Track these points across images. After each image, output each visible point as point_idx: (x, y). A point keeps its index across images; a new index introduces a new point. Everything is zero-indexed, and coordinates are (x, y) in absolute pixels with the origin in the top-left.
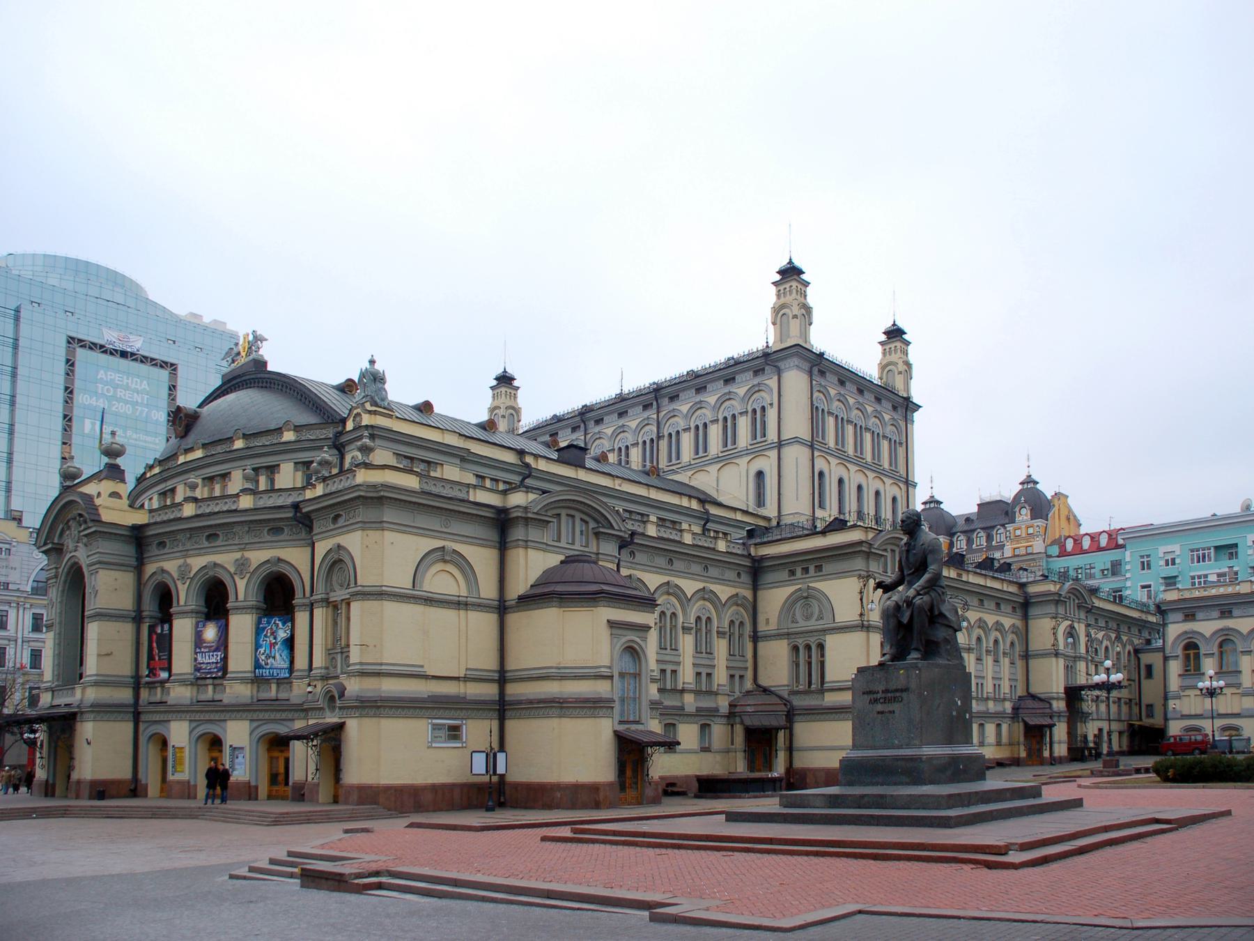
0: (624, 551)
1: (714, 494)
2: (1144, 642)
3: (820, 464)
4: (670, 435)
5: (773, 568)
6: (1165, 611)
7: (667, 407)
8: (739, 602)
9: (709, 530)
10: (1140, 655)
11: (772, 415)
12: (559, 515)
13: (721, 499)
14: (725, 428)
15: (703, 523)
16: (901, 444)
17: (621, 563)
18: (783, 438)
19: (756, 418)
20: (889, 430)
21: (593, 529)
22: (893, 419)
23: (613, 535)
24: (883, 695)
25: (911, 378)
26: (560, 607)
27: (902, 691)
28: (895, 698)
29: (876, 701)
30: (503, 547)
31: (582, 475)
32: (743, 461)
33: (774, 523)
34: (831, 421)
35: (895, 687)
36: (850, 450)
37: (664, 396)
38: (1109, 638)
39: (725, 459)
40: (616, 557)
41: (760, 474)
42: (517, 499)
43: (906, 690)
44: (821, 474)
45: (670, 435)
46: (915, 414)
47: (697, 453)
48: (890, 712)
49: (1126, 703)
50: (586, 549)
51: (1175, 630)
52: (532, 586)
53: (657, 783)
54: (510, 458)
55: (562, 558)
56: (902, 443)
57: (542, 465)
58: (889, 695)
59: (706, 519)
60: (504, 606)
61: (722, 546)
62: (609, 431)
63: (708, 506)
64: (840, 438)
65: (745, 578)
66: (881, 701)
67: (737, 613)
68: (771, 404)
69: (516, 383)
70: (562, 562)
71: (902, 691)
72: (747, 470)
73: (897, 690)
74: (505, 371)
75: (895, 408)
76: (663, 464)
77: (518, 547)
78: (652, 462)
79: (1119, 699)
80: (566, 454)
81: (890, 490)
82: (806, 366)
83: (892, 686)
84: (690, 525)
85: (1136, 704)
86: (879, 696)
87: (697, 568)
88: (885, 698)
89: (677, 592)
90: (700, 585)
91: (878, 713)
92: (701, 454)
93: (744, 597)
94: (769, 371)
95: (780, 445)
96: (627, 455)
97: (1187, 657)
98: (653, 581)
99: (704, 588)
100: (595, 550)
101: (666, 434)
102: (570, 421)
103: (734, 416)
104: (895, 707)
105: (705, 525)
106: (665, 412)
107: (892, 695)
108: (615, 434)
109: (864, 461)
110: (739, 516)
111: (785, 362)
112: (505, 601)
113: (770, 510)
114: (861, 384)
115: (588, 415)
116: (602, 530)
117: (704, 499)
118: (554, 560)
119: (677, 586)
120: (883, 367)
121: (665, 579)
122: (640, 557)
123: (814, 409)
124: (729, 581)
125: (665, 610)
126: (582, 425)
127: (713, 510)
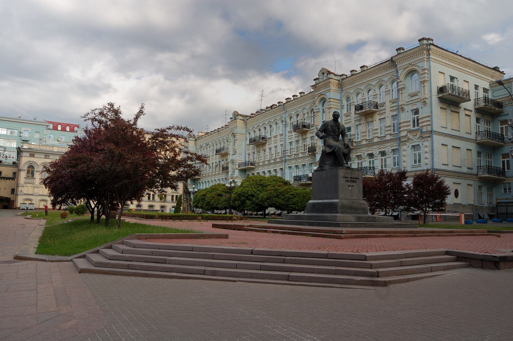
6: (22, 151)
24: (350, 179)
35: (354, 177)
43: (358, 178)
58: (352, 179)
71: (357, 178)
83: (353, 176)
86: (349, 179)
91: (349, 186)
97: (28, 172)
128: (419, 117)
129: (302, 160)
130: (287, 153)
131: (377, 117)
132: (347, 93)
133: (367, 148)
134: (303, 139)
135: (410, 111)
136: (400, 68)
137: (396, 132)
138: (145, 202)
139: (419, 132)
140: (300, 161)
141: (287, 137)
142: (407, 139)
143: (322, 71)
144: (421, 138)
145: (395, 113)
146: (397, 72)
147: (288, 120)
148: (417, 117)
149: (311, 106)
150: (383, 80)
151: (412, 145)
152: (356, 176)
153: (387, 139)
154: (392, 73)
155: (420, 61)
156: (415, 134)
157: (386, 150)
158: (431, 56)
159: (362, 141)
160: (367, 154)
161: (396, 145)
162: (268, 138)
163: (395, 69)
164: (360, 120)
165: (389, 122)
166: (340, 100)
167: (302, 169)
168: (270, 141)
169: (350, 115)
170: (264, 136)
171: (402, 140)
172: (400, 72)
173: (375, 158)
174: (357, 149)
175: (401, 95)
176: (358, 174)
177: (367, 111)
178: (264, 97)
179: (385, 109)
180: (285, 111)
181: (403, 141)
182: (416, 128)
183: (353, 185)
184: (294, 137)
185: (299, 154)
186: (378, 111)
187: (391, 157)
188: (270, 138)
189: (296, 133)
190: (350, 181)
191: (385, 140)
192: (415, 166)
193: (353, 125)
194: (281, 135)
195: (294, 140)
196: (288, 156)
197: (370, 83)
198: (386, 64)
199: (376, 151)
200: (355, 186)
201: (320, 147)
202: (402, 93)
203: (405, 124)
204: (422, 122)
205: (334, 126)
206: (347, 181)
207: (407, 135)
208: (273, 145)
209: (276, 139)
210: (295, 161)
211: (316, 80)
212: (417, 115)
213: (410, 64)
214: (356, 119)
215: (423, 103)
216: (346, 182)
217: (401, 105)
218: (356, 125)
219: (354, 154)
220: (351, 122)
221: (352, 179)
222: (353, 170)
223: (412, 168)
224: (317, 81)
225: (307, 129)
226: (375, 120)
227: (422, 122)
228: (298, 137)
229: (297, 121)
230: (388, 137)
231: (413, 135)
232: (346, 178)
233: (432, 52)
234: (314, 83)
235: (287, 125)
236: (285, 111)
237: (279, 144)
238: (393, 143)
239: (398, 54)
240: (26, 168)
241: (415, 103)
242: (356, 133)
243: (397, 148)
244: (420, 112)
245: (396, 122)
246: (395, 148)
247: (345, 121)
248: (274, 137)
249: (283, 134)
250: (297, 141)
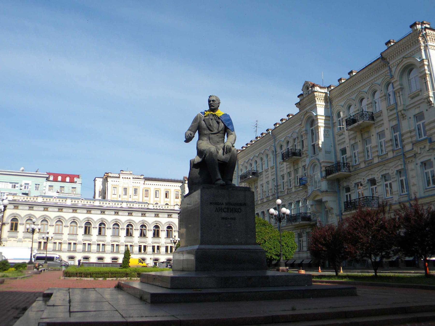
24: (227, 207)
29: (221, 210)
43: (245, 204)
48: (232, 219)
51: (8, 212)
58: (231, 207)
71: (241, 205)
86: (223, 207)
88: (228, 208)
91: (223, 218)
107: (233, 207)
128: (426, 123)
129: (296, 195)
130: (280, 188)
131: (374, 132)
132: (337, 107)
133: (367, 172)
134: (295, 170)
135: (413, 117)
136: (392, 65)
137: (400, 147)
138: (135, 255)
139: (428, 142)
140: (294, 196)
141: (278, 169)
142: (413, 154)
143: (306, 85)
144: (431, 151)
145: (394, 123)
146: (390, 69)
147: (278, 150)
148: (423, 123)
149: (300, 129)
150: (375, 84)
151: (421, 161)
153: (389, 157)
154: (385, 74)
155: (416, 51)
156: (422, 147)
157: (390, 172)
158: (429, 43)
159: (360, 164)
160: (368, 180)
161: (401, 165)
162: (260, 173)
163: (388, 68)
164: (355, 138)
165: (388, 136)
166: (330, 117)
167: (296, 206)
168: (261, 176)
169: (344, 134)
170: (256, 171)
171: (408, 156)
172: (393, 69)
173: (377, 184)
174: (356, 175)
175: (398, 98)
177: (360, 125)
178: (259, 127)
179: (382, 120)
180: (274, 140)
181: (409, 158)
182: (424, 137)
184: (285, 168)
185: (292, 188)
186: (374, 124)
187: (397, 180)
188: (261, 173)
189: (288, 163)
191: (387, 158)
192: (429, 190)
193: (348, 145)
194: (272, 168)
195: (285, 172)
196: (281, 192)
197: (362, 91)
198: (375, 63)
199: (377, 174)
201: (312, 177)
202: (399, 96)
203: (409, 135)
204: (431, 129)
205: (210, 120)
207: (413, 149)
208: (265, 181)
209: (268, 173)
210: (288, 197)
211: (300, 97)
212: (423, 121)
213: (403, 58)
214: (351, 137)
215: (427, 103)
217: (401, 111)
218: (352, 145)
219: (352, 182)
220: (345, 141)
223: (424, 192)
224: (302, 97)
225: (297, 157)
226: (373, 135)
227: (431, 129)
228: (290, 168)
229: (288, 148)
230: (390, 155)
231: (421, 148)
232: (217, 204)
233: (430, 38)
234: (298, 100)
235: (278, 155)
236: (274, 140)
237: (270, 178)
238: (397, 161)
239: (389, 48)
240: (9, 221)
241: (418, 106)
242: (352, 154)
243: (403, 167)
244: (426, 116)
245: (397, 134)
246: (400, 168)
247: (338, 141)
248: (265, 170)
249: (274, 166)
250: (289, 174)
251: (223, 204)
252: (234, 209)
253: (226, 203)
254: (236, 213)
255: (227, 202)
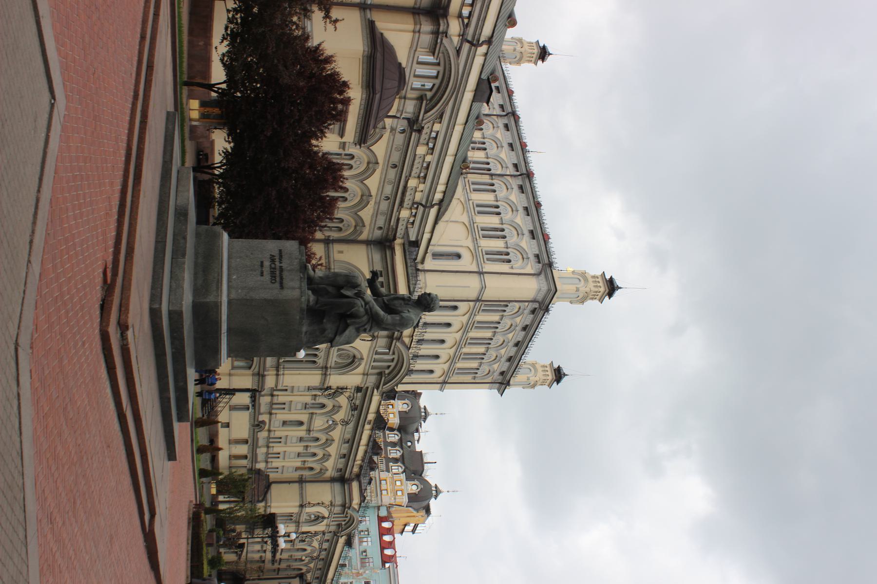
0: (406, 122)
1: (446, 217)
2: (308, 581)
3: (463, 307)
4: (493, 185)
5: (384, 259)
7: (515, 183)
8: (358, 228)
9: (417, 208)
10: (298, 579)
11: (505, 268)
12: (439, 64)
13: (441, 225)
14: (496, 230)
15: (424, 203)
16: (474, 378)
17: (396, 120)
18: (486, 275)
19: (502, 255)
20: (485, 368)
21: (426, 95)
22: (494, 372)
23: (419, 113)
24: (278, 267)
25: (524, 388)
26: (363, 57)
27: (281, 284)
28: (275, 277)
30: (415, 12)
31: (468, 96)
32: (469, 243)
33: (420, 267)
34: (495, 317)
35: (284, 277)
36: (473, 334)
37: (523, 181)
38: (313, 551)
39: (470, 227)
40: (401, 115)
41: (458, 256)
42: (454, 27)
43: (282, 287)
44: (455, 308)
45: (493, 185)
46: (496, 390)
47: (478, 206)
49: (260, 567)
50: (409, 88)
52: (382, 34)
53: (208, 137)
54: (487, 31)
55: (404, 65)
56: (474, 379)
57: (479, 61)
58: (278, 273)
59: (427, 206)
60: (366, 9)
61: (405, 214)
62: (499, 135)
63: (436, 208)
64: (483, 325)
65: (378, 233)
66: (273, 266)
67: (349, 226)
68: (512, 268)
69: (540, 62)
70: (400, 64)
71: (281, 284)
72: (462, 246)
73: (281, 278)
74: (550, 54)
75: (502, 373)
76: (472, 178)
77: (415, 24)
78: (473, 169)
79: (264, 562)
80: (485, 86)
81: (439, 367)
82: (540, 298)
83: (285, 274)
84: (422, 191)
85: (259, 576)
86: (277, 263)
87: (388, 190)
88: (275, 268)
89: (369, 170)
90: (373, 193)
91: (262, 263)
92: (477, 209)
93: (361, 233)
94: (537, 267)
95: (481, 273)
96: (479, 149)
98: (380, 149)
99: (371, 196)
100: (409, 96)
101: (494, 182)
102: (508, 104)
103: (504, 237)
104: (267, 277)
105: (421, 204)
106: (511, 182)
108: (495, 141)
109: (463, 346)
110: (426, 236)
111: (544, 280)
112: (370, 10)
113: (430, 264)
114: (521, 346)
115: (512, 119)
116: (424, 102)
117: (443, 205)
118: (402, 56)
119: (374, 171)
120: (533, 365)
121: (380, 161)
122: (400, 139)
123: (506, 303)
124: (376, 220)
125: (355, 160)
126: (504, 113)
127: (433, 211)
152: (288, 283)
176: (293, 288)
183: (265, 273)
190: (273, 266)
200: (262, 278)
206: (272, 259)
216: (269, 256)
221: (278, 273)
222: (301, 278)
251: (281, 263)
252: (275, 275)
253: (282, 266)
254: (270, 277)
255: (283, 268)
